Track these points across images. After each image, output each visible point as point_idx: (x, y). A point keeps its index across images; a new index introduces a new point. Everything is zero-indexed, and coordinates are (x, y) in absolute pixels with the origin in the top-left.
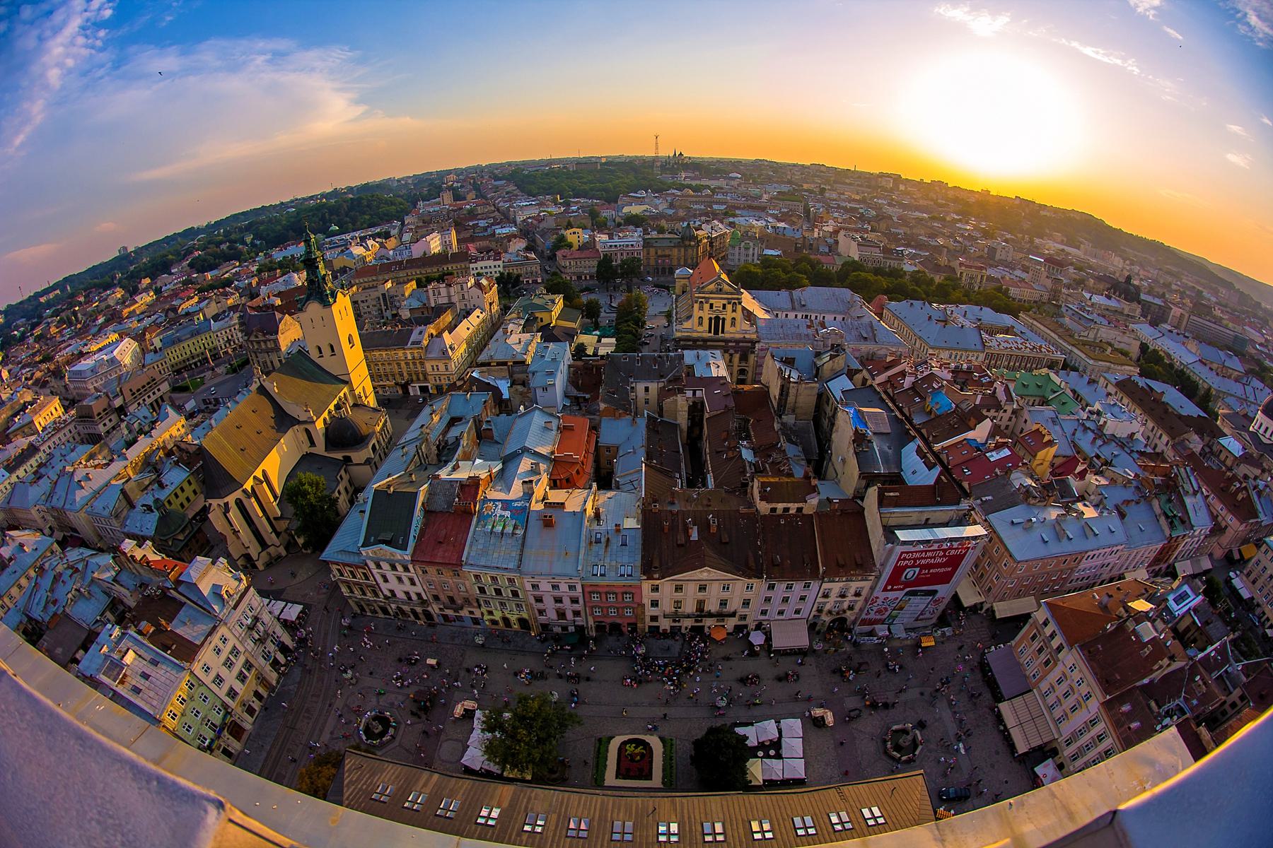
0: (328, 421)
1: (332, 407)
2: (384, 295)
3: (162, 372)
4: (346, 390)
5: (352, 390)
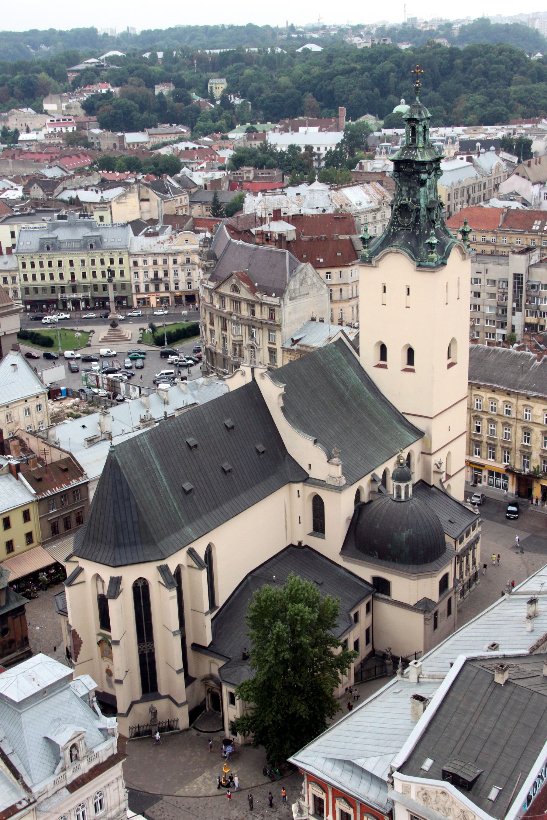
0: (364, 498)
1: (379, 471)
2: (518, 277)
3: (11, 294)
4: (416, 448)
5: (425, 453)
